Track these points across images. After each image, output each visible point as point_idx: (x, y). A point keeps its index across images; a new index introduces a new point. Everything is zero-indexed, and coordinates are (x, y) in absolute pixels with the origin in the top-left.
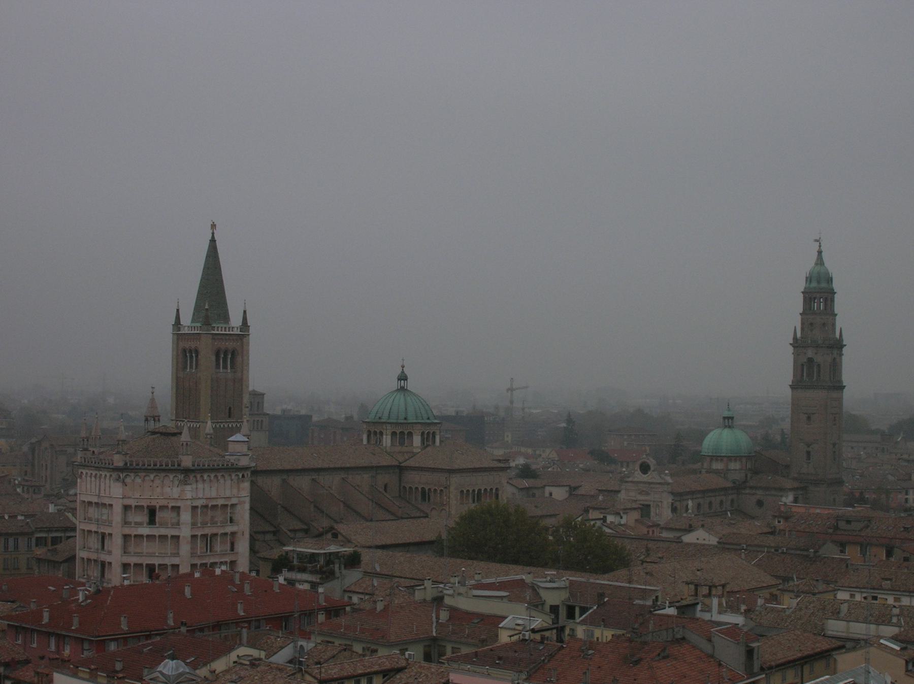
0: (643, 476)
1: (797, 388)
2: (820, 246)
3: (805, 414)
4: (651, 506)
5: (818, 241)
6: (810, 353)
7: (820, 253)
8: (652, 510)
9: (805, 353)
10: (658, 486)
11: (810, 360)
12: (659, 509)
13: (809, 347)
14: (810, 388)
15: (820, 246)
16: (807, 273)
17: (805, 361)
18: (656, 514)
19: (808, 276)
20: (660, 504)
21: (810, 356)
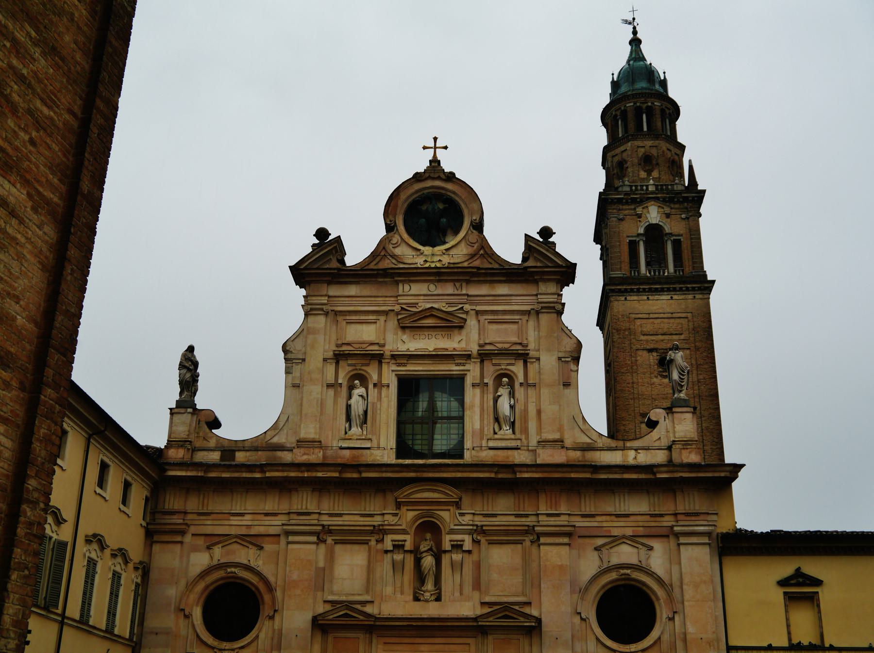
0: (427, 250)
1: (626, 291)
2: (635, 32)
3: (650, 351)
4: (469, 381)
5: (630, 23)
6: (653, 214)
7: (635, 42)
8: (472, 396)
9: (640, 216)
10: (503, 289)
11: (654, 233)
12: (512, 394)
13: (649, 199)
14: (662, 290)
15: (635, 32)
16: (613, 74)
17: (641, 231)
18: (497, 420)
19: (615, 79)
20: (518, 369)
21: (654, 222)
